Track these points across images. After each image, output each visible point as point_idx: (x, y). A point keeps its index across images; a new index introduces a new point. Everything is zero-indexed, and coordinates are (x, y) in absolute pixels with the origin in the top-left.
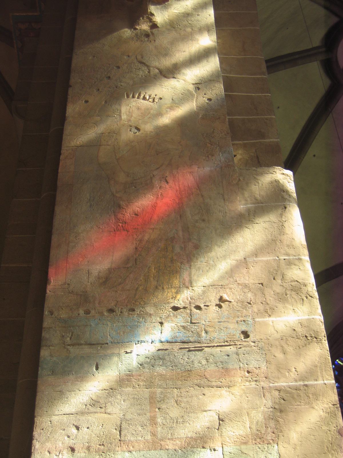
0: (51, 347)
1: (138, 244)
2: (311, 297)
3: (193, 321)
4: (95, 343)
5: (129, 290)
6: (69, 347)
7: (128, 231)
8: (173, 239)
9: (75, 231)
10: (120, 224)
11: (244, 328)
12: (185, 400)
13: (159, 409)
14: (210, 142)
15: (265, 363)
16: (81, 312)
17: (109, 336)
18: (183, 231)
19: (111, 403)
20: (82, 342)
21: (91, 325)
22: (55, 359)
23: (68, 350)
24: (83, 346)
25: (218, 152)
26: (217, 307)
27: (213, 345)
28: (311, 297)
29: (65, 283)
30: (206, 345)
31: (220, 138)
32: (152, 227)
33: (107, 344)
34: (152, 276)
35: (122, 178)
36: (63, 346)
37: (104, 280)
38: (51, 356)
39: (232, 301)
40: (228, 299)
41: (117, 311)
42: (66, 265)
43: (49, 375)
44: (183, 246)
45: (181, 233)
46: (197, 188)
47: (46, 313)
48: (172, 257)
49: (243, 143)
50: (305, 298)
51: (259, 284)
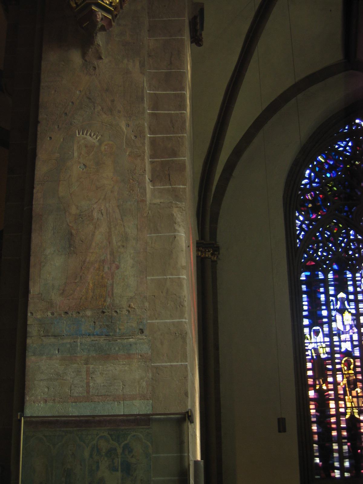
0: (33, 338)
1: (82, 264)
2: (182, 306)
3: (113, 322)
4: (57, 335)
5: (76, 299)
6: (42, 338)
7: (77, 254)
8: (104, 261)
9: (44, 253)
10: (72, 249)
11: (141, 327)
12: (105, 372)
13: (91, 378)
14: (132, 179)
15: (150, 351)
16: (49, 314)
17: (65, 331)
18: (110, 254)
19: (66, 374)
20: (50, 335)
21: (54, 323)
22: (35, 345)
24: (50, 337)
25: (137, 188)
26: (127, 312)
27: (123, 337)
28: (182, 306)
29: (39, 294)
30: (118, 338)
31: (139, 175)
32: (91, 251)
33: (64, 336)
34: (90, 288)
35: (73, 210)
36: (39, 337)
37: (62, 291)
38: (33, 343)
39: (136, 308)
40: (133, 307)
41: (69, 314)
42: (40, 280)
43: (32, 356)
44: (109, 267)
45: (109, 256)
46: (121, 219)
47: (29, 314)
48: (103, 275)
49: (161, 160)
50: (178, 307)
51: (153, 296)
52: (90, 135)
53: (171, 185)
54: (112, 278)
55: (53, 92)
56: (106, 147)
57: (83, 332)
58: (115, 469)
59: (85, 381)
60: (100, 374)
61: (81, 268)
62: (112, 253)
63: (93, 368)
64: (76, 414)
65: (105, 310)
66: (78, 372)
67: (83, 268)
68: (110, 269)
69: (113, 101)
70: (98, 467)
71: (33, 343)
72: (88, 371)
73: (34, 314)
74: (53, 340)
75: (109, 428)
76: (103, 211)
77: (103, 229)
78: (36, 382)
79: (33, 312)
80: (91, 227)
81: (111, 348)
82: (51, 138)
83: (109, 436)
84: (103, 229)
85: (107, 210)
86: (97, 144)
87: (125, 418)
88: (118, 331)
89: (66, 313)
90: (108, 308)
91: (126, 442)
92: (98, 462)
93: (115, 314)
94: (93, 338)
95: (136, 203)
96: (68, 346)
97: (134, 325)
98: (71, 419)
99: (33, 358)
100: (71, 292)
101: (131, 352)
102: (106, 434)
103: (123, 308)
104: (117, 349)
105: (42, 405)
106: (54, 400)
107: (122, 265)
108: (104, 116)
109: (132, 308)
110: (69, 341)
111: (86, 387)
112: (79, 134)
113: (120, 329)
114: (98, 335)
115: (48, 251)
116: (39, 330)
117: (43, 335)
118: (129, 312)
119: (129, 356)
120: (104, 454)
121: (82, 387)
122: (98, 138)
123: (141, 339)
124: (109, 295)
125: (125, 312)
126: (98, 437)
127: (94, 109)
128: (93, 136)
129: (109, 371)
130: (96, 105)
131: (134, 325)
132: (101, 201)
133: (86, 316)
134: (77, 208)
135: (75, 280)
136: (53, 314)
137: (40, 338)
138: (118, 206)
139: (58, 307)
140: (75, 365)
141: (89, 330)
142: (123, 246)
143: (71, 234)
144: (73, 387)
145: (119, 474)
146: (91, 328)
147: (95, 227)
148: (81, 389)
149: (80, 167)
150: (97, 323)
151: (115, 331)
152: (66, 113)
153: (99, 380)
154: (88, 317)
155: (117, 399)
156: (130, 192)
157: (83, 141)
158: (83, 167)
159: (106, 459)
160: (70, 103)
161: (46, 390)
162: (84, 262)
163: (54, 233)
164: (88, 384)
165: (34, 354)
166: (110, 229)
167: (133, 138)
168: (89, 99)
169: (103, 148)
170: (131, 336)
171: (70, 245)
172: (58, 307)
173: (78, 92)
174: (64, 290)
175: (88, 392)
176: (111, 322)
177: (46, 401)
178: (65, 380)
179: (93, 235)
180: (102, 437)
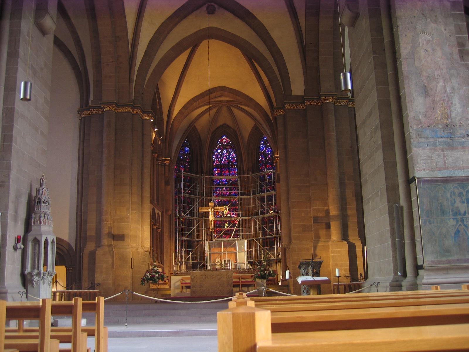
8: (444, 100)
11: (467, 133)
16: (420, 127)
18: (447, 97)
20: (422, 137)
23: (418, 140)
32: (437, 95)
35: (424, 74)
38: (414, 141)
40: (462, 123)
45: (446, 98)
52: (427, 34)
53: (464, 62)
54: (450, 109)
55: (403, 10)
56: (436, 41)
57: (439, 136)
58: (464, 202)
59: (443, 160)
60: (450, 156)
61: (433, 104)
62: (448, 96)
63: (446, 153)
64: (441, 176)
65: (448, 125)
66: (439, 156)
67: (434, 104)
68: (448, 104)
69: (436, 16)
70: (455, 202)
71: (414, 141)
72: (444, 155)
73: (412, 127)
74: (423, 140)
75: (458, 183)
76: (440, 74)
77: (441, 83)
78: (418, 161)
79: (412, 126)
80: (435, 82)
81: (454, 144)
82: (406, 35)
83: (459, 187)
84: (441, 83)
85: (442, 74)
86: (431, 39)
87: (465, 178)
88: (456, 135)
89: (428, 126)
90: (449, 124)
91: (467, 189)
92: (455, 199)
93: (454, 127)
94: (444, 139)
95: (456, 71)
96: (432, 143)
97: (464, 132)
98: (438, 178)
99: (415, 149)
100: (430, 116)
101: (464, 146)
102: (457, 185)
103: (457, 124)
104: (457, 144)
105: (423, 172)
106: (429, 169)
107: (454, 102)
108: (432, 24)
109: (461, 124)
110: (432, 140)
111: (444, 163)
112: (421, 34)
113: (457, 135)
114: (446, 137)
115: (414, 95)
116: (416, 135)
117: (418, 137)
118: (460, 125)
119: (463, 148)
120: (457, 195)
121: (442, 163)
122: (431, 36)
123: (468, 139)
124: (449, 117)
125: (458, 126)
126: (453, 187)
127: (427, 20)
128: (428, 35)
129: (454, 155)
130: (427, 18)
131: (464, 132)
132: (438, 69)
133: (439, 128)
134: (426, 73)
135: (431, 109)
136: (422, 127)
137: (417, 139)
138: (447, 72)
139: (424, 123)
140: (437, 152)
141: (442, 135)
142: (453, 93)
143: (425, 86)
144: (437, 163)
145: (466, 204)
146: (442, 134)
147: (437, 83)
148: (442, 164)
149: (424, 51)
150: (445, 131)
151: (455, 135)
152: (412, 22)
153: (450, 159)
154: (440, 128)
155: (460, 168)
156: (452, 65)
157: (423, 37)
158: (425, 51)
159: (458, 197)
160: (413, 17)
161: (424, 165)
162: (434, 100)
163: (416, 85)
164: (445, 161)
165: (415, 147)
166: (444, 83)
167: (449, 37)
168: (423, 14)
169: (434, 42)
170: (463, 138)
171: (426, 92)
172: (424, 123)
173: (416, 11)
174: (426, 115)
175: (445, 165)
176: (452, 131)
177: (424, 170)
178: (433, 160)
179: (437, 87)
180: (455, 187)
